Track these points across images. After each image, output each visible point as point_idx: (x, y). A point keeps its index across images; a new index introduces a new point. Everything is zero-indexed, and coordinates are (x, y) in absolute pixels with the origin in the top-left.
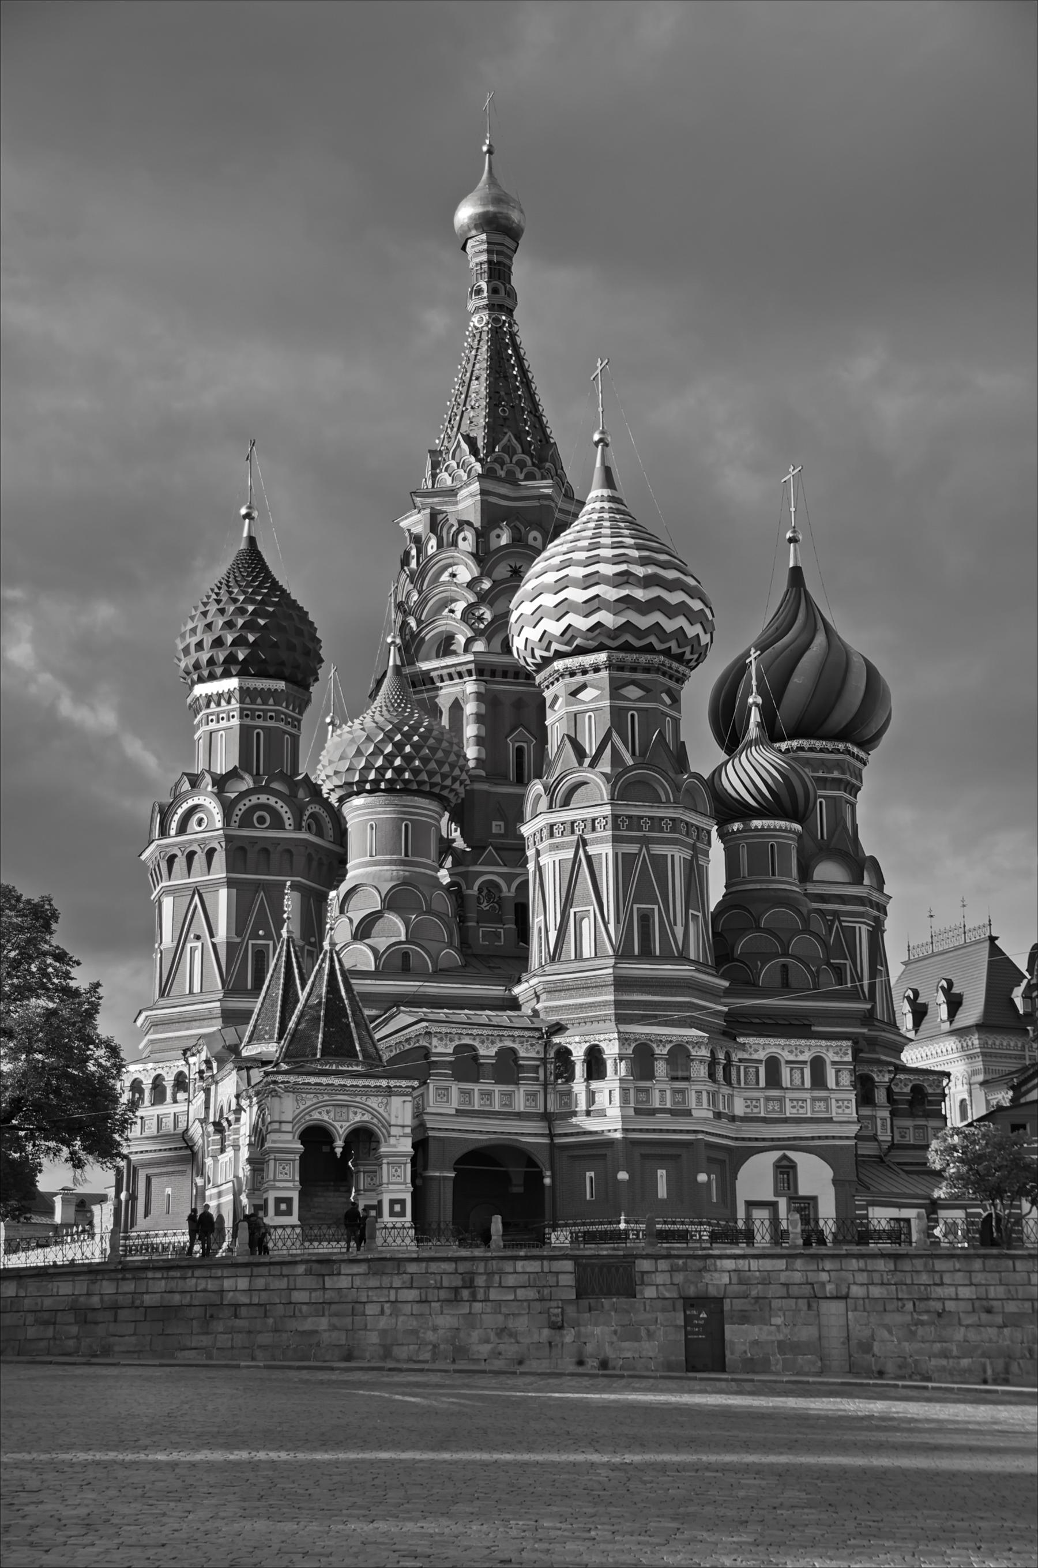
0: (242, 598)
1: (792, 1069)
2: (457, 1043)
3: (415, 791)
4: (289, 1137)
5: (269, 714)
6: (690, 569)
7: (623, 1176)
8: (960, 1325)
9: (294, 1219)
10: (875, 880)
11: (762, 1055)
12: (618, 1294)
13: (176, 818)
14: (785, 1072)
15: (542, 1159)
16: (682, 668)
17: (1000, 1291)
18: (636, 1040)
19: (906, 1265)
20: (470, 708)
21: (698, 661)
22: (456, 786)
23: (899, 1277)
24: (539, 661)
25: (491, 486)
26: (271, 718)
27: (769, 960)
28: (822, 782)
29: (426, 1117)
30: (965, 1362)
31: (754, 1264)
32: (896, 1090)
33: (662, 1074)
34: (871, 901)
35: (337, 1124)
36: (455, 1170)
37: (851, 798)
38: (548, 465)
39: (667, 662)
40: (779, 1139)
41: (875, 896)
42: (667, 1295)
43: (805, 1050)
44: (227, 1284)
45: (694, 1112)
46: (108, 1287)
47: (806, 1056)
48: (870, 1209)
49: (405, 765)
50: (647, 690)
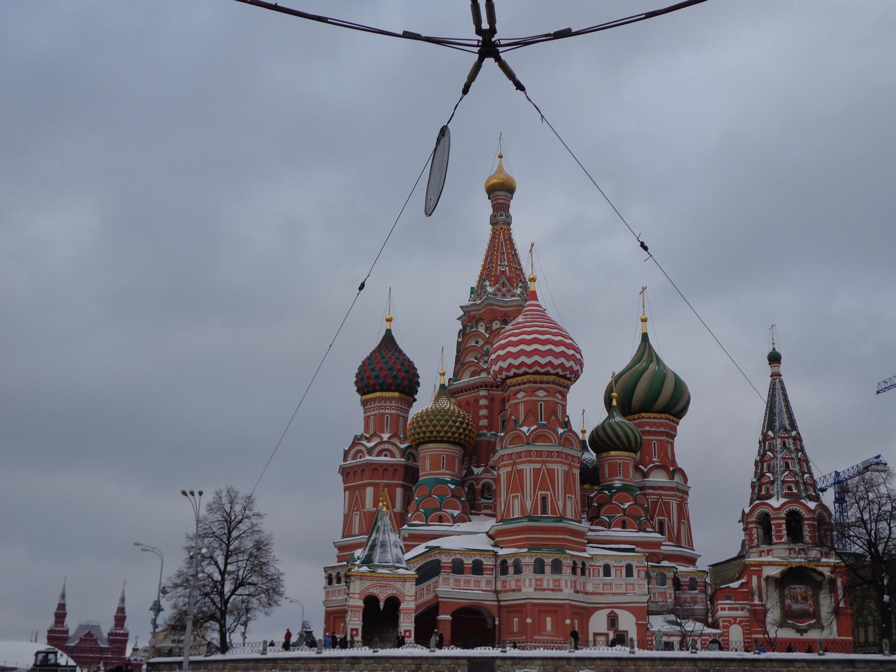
0: (380, 357)
1: (616, 570)
2: (453, 557)
5: (392, 408)
6: (571, 335)
7: (529, 620)
10: (682, 479)
14: (613, 571)
15: (495, 612)
16: (566, 382)
20: (483, 402)
26: (393, 409)
32: (682, 580)
33: (548, 572)
35: (380, 594)
36: (451, 616)
37: (671, 440)
39: (557, 378)
40: (609, 603)
47: (624, 563)
49: (441, 430)
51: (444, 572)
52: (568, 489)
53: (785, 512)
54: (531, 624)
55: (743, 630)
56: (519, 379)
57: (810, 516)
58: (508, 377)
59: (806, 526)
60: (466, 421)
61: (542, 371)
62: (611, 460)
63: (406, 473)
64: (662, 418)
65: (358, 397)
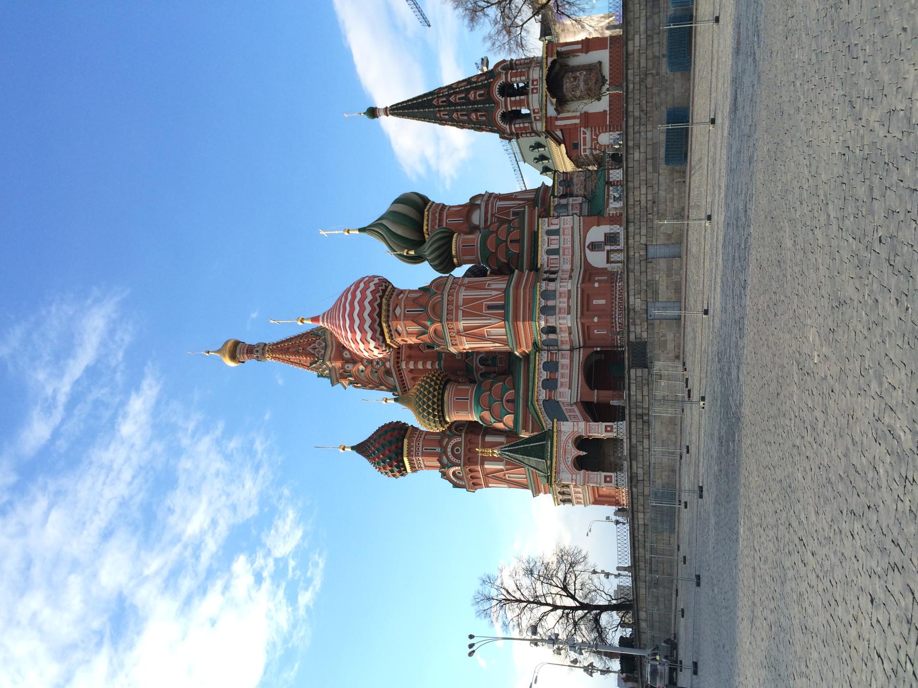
4: (578, 476)
6: (348, 286)
7: (596, 320)
8: (658, 193)
9: (612, 474)
11: (545, 257)
12: (645, 349)
13: (458, 482)
14: (552, 247)
15: (589, 351)
16: (388, 290)
17: (643, 174)
18: (539, 314)
19: (631, 217)
20: (411, 366)
23: (637, 221)
24: (388, 348)
25: (327, 357)
27: (509, 248)
28: (441, 220)
29: (572, 403)
30: (676, 191)
31: (631, 287)
37: (447, 208)
38: (320, 333)
39: (385, 297)
40: (581, 250)
41: (485, 198)
42: (646, 327)
43: (543, 239)
44: (641, 522)
46: (642, 573)
47: (546, 238)
50: (397, 305)
51: (554, 397)
53: (500, 98)
54: (599, 317)
55: (603, 132)
57: (504, 76)
59: (514, 79)
60: (425, 379)
61: (378, 310)
63: (472, 432)
65: (410, 475)
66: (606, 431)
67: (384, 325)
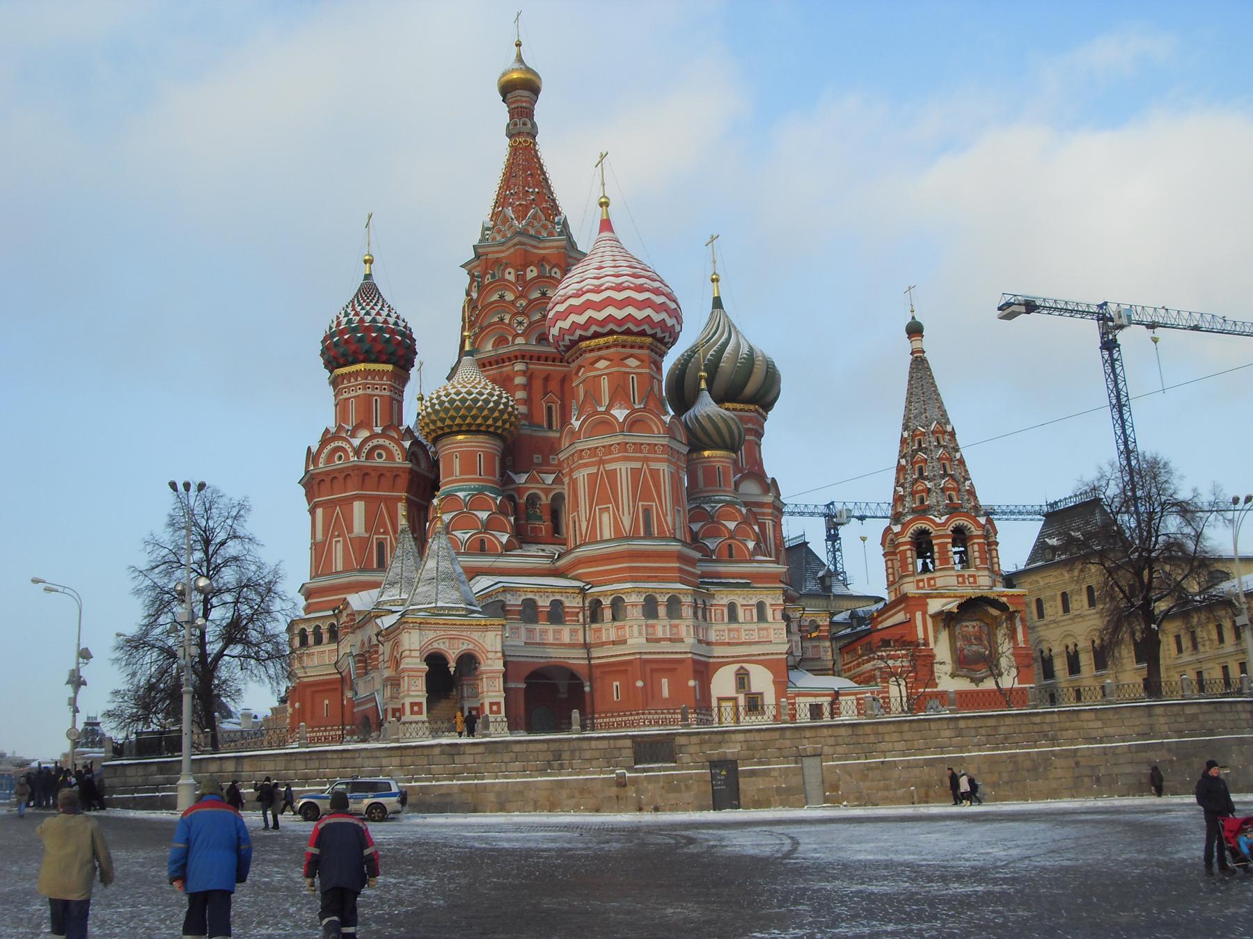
0: (363, 312)
1: (745, 610)
3: (484, 432)
7: (640, 684)
9: (424, 717)
11: (725, 601)
15: (583, 674)
16: (663, 348)
19: (860, 731)
21: (673, 344)
22: (513, 428)
24: (567, 343)
26: (385, 389)
31: (757, 736)
34: (774, 506)
35: (451, 652)
39: (655, 343)
45: (685, 640)
47: (754, 601)
48: (797, 699)
50: (642, 361)
52: (676, 501)
53: (951, 528)
56: (602, 341)
57: (980, 533)
58: (582, 338)
59: (976, 548)
61: (635, 329)
62: (705, 462)
63: (411, 482)
64: (751, 411)
66: (491, 704)
67: (611, 339)
